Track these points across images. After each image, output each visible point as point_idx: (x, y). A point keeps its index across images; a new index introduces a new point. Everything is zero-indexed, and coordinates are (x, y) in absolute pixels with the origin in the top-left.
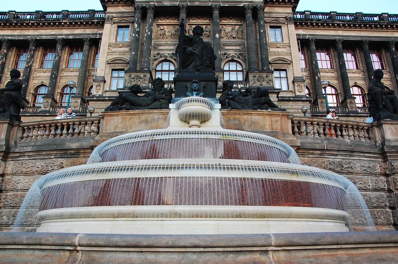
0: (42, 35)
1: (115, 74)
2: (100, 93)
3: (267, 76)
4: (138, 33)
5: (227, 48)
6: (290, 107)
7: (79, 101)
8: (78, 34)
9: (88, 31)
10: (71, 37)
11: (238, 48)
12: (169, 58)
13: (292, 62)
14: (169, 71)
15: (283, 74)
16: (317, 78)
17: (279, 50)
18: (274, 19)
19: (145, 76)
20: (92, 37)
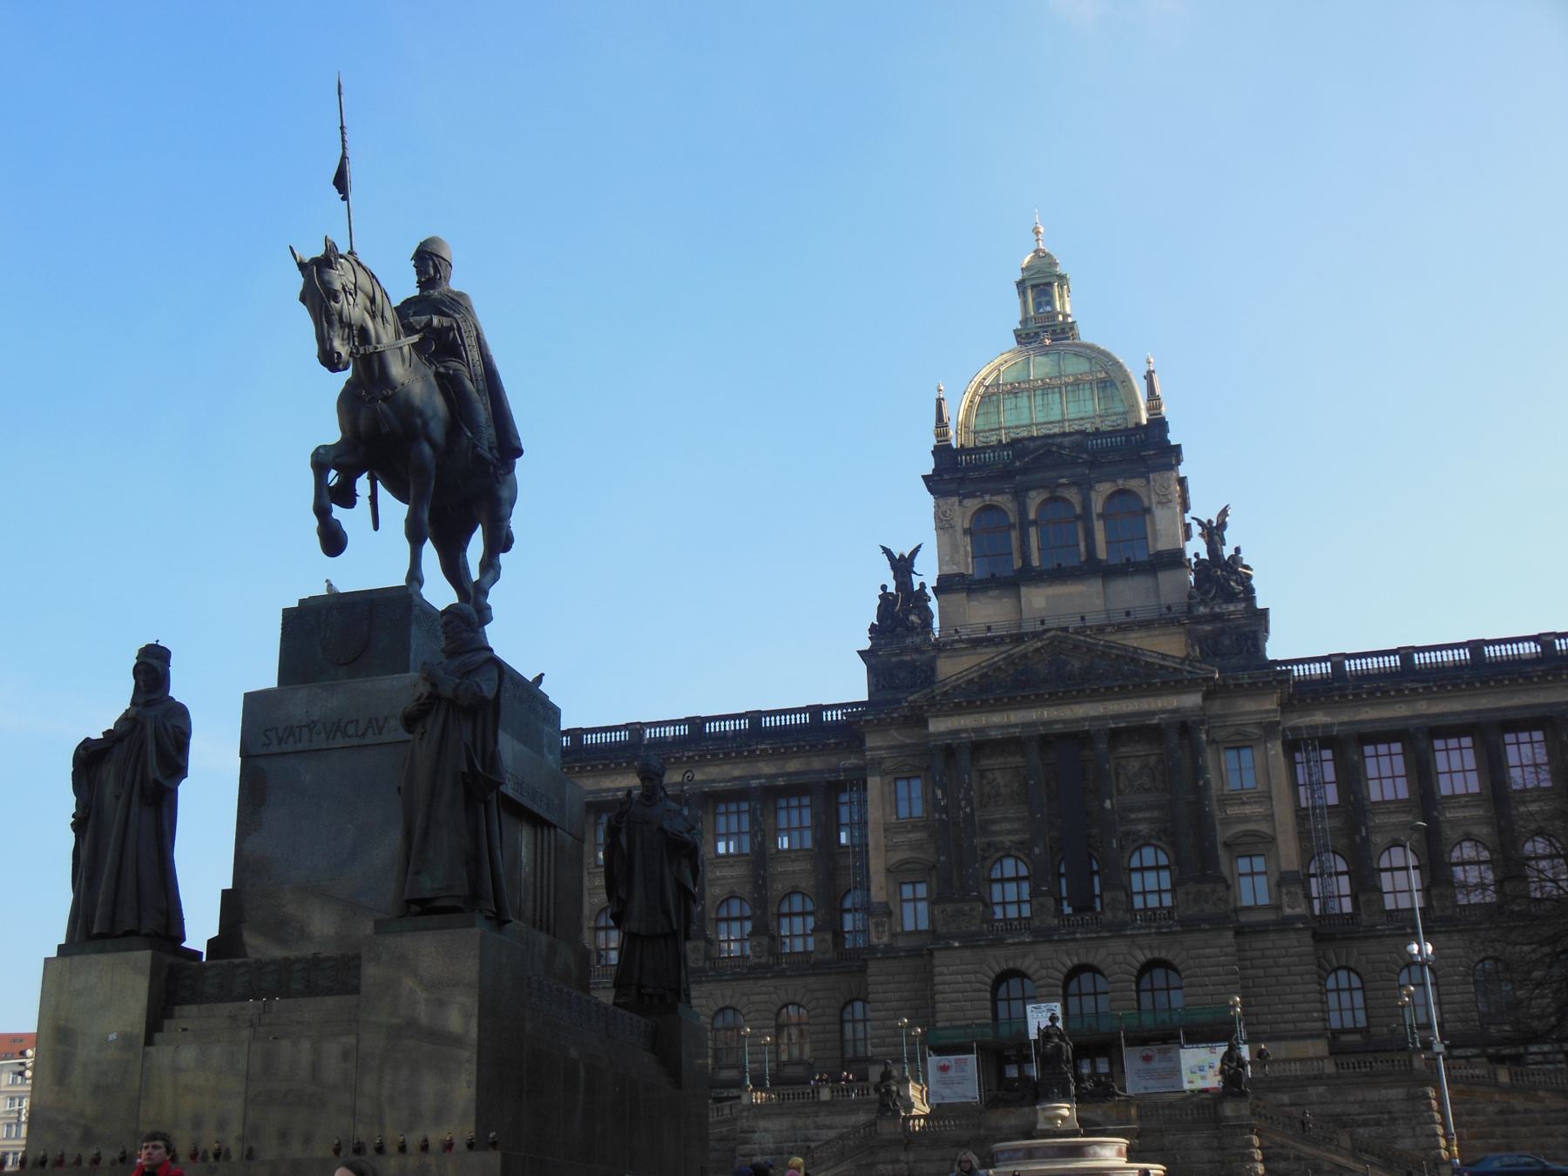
0: (714, 781)
1: (907, 891)
2: (885, 939)
3: (1213, 891)
4: (945, 809)
5: (1133, 816)
6: (1270, 945)
7: (829, 937)
8: (796, 773)
9: (818, 763)
10: (781, 782)
11: (1156, 814)
12: (1013, 852)
13: (1273, 840)
14: (1017, 879)
15: (1259, 864)
16: (1358, 839)
17: (1248, 810)
18: (1233, 730)
19: (972, 909)
20: (831, 777)
